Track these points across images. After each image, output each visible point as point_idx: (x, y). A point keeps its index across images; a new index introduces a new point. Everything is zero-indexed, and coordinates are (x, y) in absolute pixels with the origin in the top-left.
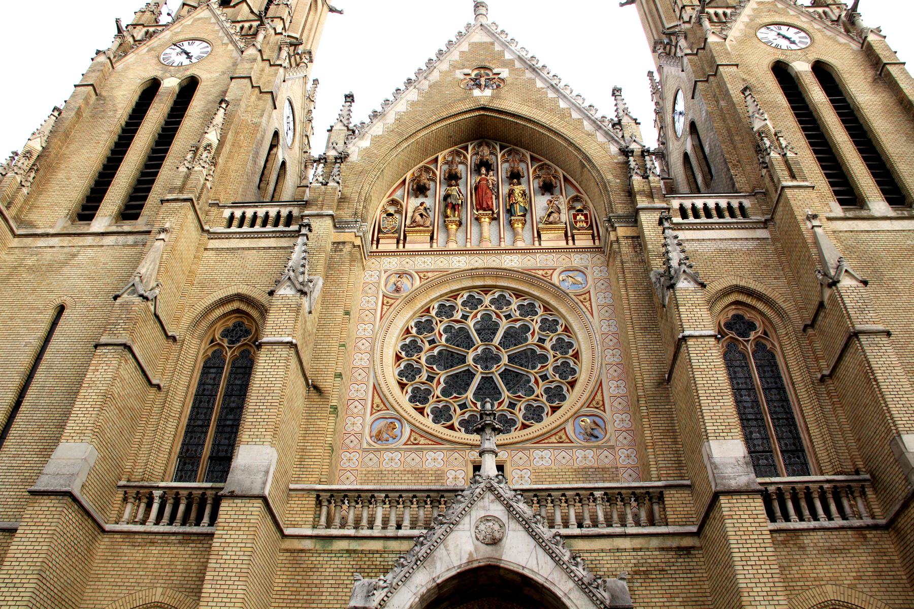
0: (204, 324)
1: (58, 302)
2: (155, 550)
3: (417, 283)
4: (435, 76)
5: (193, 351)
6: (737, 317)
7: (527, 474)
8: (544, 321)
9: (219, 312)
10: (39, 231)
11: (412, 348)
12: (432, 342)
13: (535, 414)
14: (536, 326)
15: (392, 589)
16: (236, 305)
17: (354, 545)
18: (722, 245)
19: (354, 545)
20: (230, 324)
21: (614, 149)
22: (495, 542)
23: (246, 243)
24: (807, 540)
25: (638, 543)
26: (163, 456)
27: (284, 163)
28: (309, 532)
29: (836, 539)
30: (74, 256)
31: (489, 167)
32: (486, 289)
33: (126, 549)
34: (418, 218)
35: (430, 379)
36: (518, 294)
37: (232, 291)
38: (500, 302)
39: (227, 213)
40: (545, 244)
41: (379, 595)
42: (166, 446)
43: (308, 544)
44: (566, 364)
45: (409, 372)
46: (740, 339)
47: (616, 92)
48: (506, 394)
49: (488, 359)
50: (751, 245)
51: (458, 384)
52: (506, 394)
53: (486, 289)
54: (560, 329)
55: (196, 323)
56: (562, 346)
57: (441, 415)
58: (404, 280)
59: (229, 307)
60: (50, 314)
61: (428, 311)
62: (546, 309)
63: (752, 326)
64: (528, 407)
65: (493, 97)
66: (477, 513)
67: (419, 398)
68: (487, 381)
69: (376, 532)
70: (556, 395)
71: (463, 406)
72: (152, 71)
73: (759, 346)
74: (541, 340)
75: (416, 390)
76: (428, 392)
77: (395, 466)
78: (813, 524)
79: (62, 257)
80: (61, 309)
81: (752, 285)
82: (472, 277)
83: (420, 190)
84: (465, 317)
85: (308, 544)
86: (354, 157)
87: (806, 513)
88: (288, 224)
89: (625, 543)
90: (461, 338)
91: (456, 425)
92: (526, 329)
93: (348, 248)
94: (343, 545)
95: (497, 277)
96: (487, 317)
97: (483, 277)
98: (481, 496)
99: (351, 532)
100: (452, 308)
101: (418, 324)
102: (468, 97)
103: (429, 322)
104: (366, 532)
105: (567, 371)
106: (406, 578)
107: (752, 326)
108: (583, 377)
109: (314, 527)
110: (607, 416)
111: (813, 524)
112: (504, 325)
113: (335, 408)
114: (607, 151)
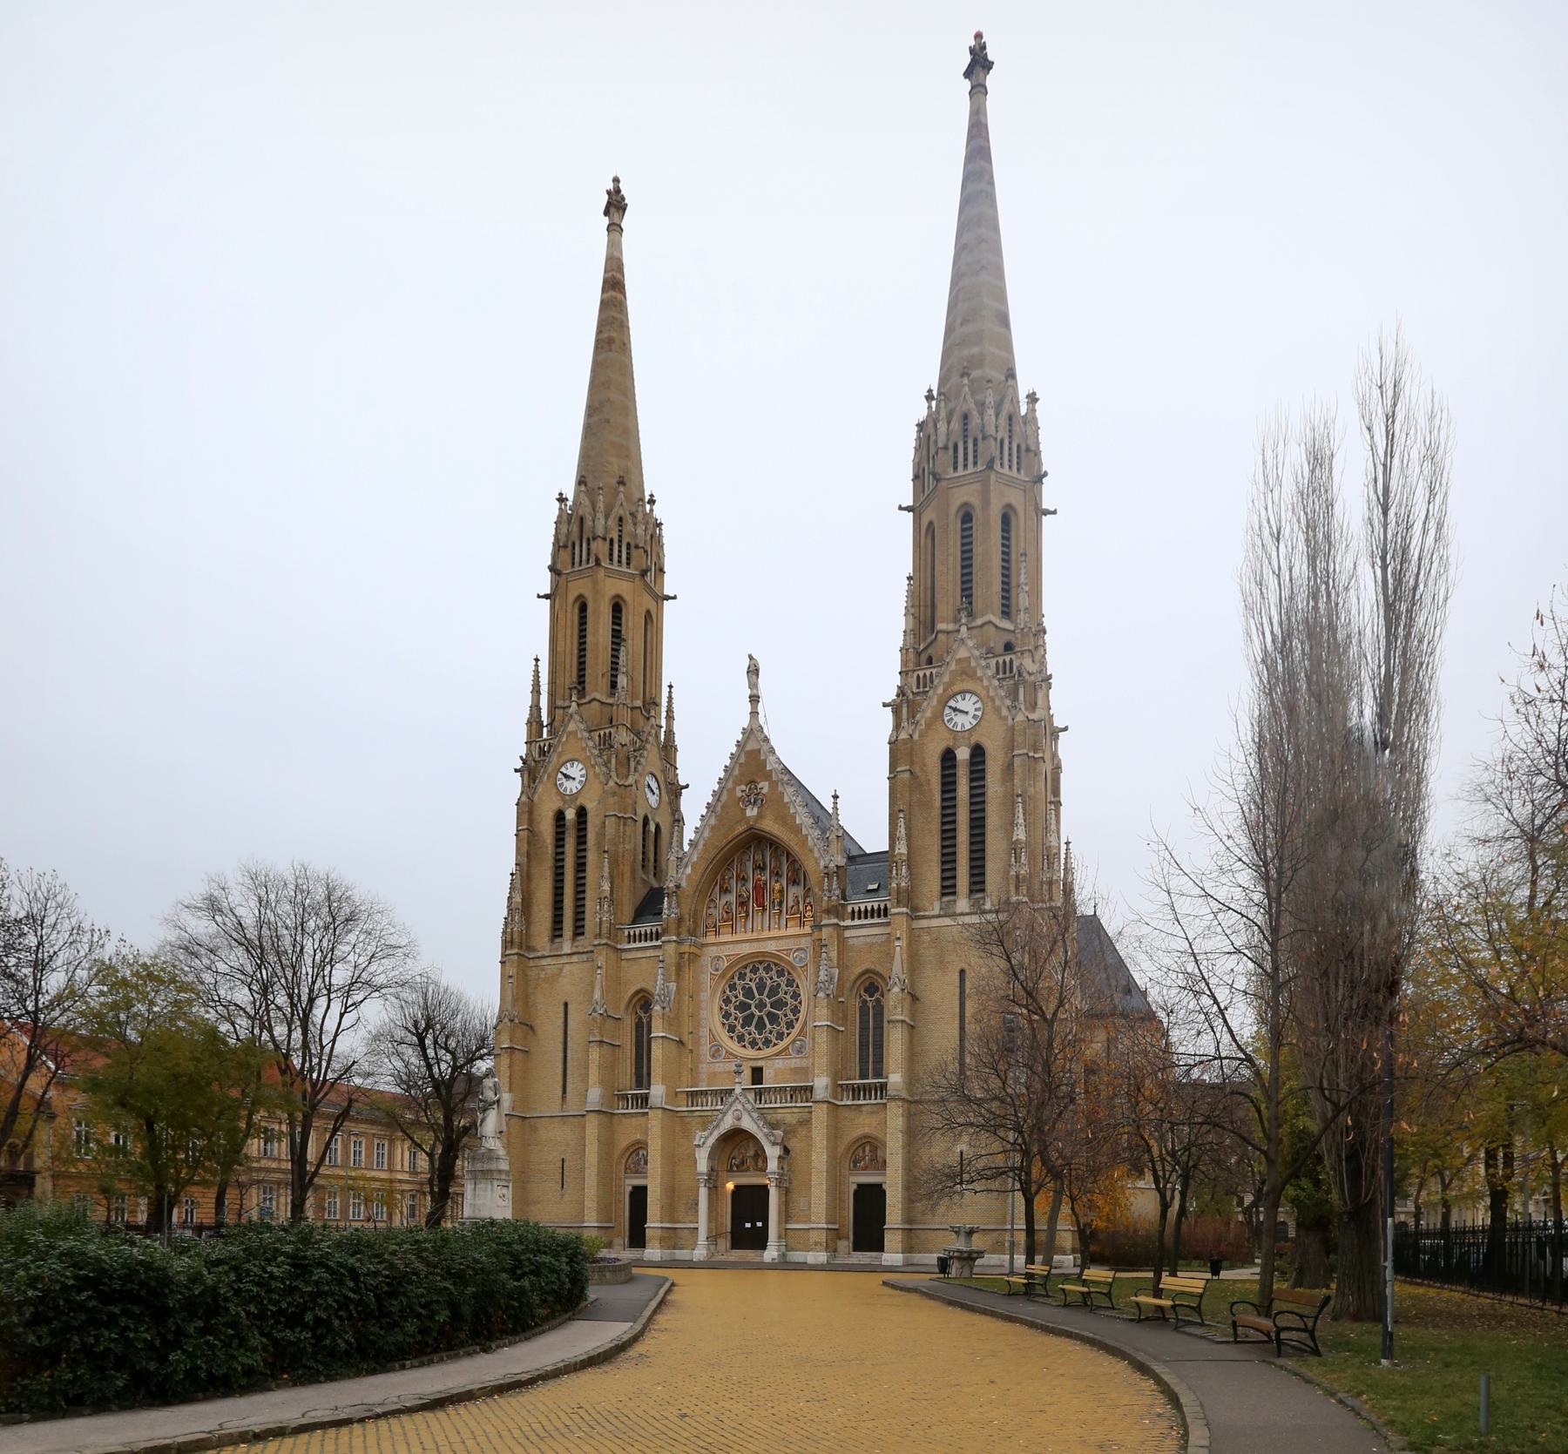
0: (631, 1007)
1: (563, 1001)
2: (633, 1119)
3: (726, 965)
4: (724, 798)
5: (629, 1023)
6: (872, 984)
7: (772, 1071)
8: (788, 980)
9: (636, 999)
10: (539, 954)
11: (727, 1001)
12: (736, 997)
13: (780, 1036)
14: (783, 986)
15: (707, 1138)
16: (640, 995)
17: (702, 1114)
18: (868, 940)
19: (702, 1114)
20: (642, 1002)
21: (822, 863)
22: (739, 1119)
23: (639, 954)
24: (864, 1108)
25: (801, 1110)
26: (629, 1077)
27: (658, 827)
28: (685, 1109)
29: (875, 1108)
30: (561, 970)
31: (762, 869)
32: (761, 962)
33: (624, 1120)
34: (725, 915)
35: (736, 1019)
36: (776, 965)
37: (639, 986)
38: (768, 969)
39: (626, 934)
40: (790, 931)
41: (702, 1140)
42: (629, 1071)
43: (686, 1114)
44: (796, 1007)
45: (727, 1015)
46: (869, 999)
47: (835, 797)
48: (769, 1026)
49: (761, 1006)
50: (885, 937)
51: (747, 1021)
52: (769, 1026)
53: (761, 962)
54: (747, 1045)
55: (627, 1008)
56: (796, 996)
57: (741, 1039)
58: (720, 962)
59: (640, 995)
60: (562, 1008)
61: (721, 1008)
62: (789, 973)
63: (877, 989)
64: (778, 1033)
65: (760, 816)
66: (733, 1108)
67: (732, 1029)
68: (761, 1018)
69: (708, 1108)
70: (790, 1025)
71: (750, 1034)
72: (557, 805)
73: (878, 1001)
74: (786, 993)
75: (730, 1026)
76: (735, 1026)
77: (720, 1070)
78: (868, 1102)
79: (556, 971)
80: (566, 1004)
81: (879, 969)
82: (753, 958)
83: (725, 890)
84: (751, 980)
85: (686, 1114)
86: (684, 884)
87: (867, 1096)
88: (657, 940)
89: (796, 1110)
90: (748, 993)
91: (747, 1045)
92: (779, 985)
93: (686, 956)
94: (697, 1114)
95: (764, 956)
96: (761, 979)
97: (758, 957)
98: (734, 1102)
99: (699, 1108)
100: (745, 974)
101: (724, 1001)
102: (744, 818)
103: (735, 984)
104: (705, 1108)
105: (796, 1011)
106: (711, 1134)
107: (877, 989)
108: (801, 1016)
109: (687, 1106)
110: (806, 1040)
111: (868, 1102)
112: (769, 982)
113: (691, 1051)
114: (818, 864)
